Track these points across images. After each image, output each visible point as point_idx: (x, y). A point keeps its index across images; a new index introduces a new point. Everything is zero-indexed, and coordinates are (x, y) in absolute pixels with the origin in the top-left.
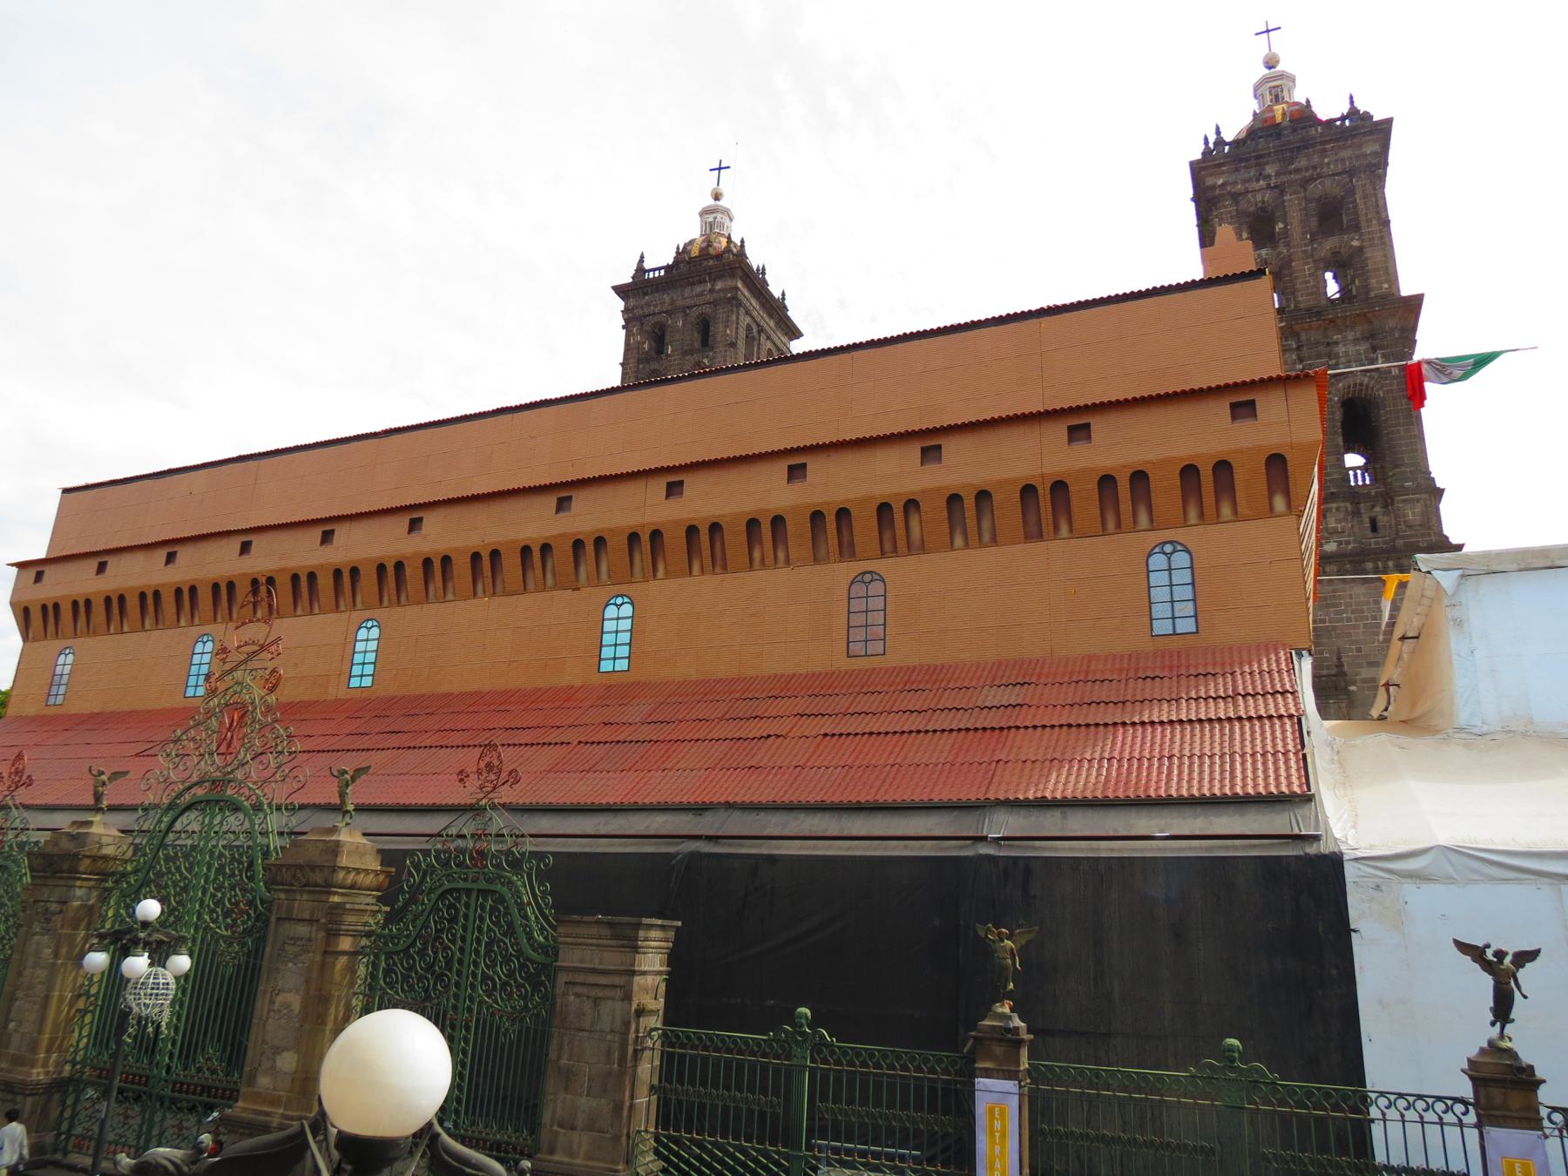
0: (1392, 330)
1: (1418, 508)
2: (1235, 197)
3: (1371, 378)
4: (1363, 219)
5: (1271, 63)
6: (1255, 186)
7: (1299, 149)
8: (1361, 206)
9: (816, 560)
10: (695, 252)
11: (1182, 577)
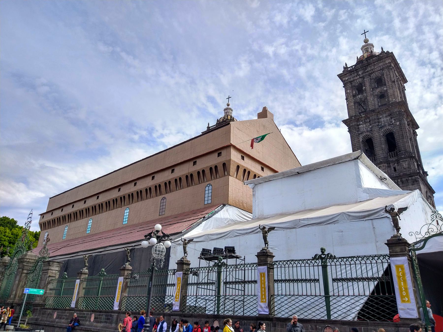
0: (396, 112)
1: (407, 163)
2: (351, 82)
3: (391, 127)
4: (386, 82)
6: (356, 78)
7: (367, 66)
9: (156, 196)
10: (221, 121)
11: (210, 191)
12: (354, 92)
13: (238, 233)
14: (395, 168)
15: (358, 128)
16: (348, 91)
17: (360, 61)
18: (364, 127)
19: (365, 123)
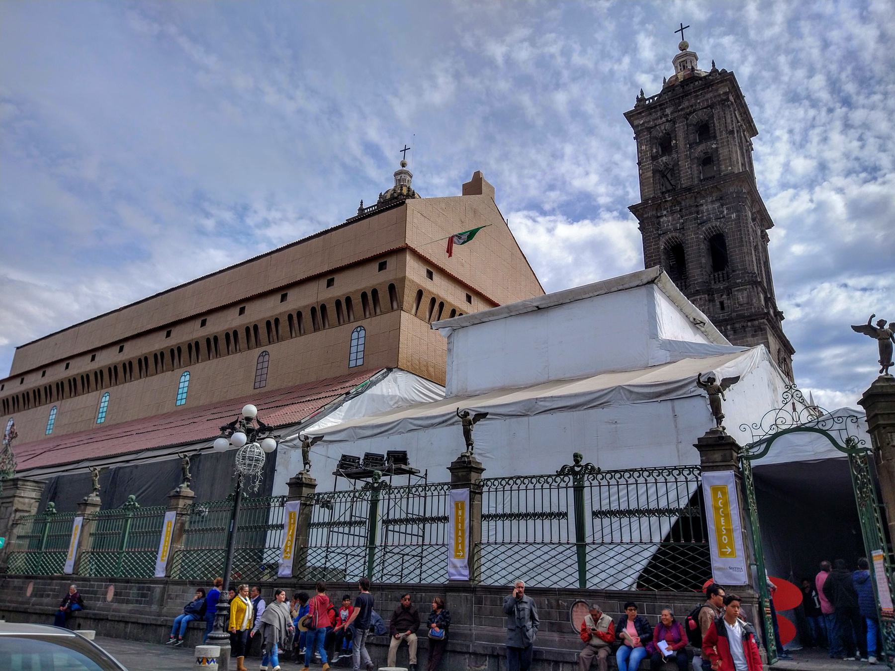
0: (732, 193)
2: (649, 129)
5: (683, 47)
6: (660, 121)
7: (682, 97)
8: (717, 124)
9: (249, 348)
10: (388, 196)
11: (362, 341)
12: (655, 150)
13: (415, 425)
14: (722, 303)
15: (659, 223)
16: (644, 147)
17: (669, 87)
18: (669, 221)
19: (672, 213)
